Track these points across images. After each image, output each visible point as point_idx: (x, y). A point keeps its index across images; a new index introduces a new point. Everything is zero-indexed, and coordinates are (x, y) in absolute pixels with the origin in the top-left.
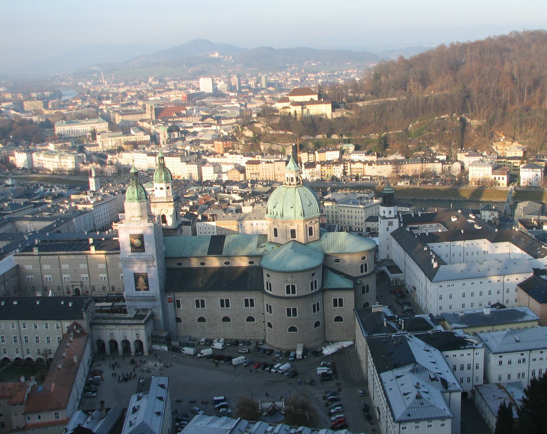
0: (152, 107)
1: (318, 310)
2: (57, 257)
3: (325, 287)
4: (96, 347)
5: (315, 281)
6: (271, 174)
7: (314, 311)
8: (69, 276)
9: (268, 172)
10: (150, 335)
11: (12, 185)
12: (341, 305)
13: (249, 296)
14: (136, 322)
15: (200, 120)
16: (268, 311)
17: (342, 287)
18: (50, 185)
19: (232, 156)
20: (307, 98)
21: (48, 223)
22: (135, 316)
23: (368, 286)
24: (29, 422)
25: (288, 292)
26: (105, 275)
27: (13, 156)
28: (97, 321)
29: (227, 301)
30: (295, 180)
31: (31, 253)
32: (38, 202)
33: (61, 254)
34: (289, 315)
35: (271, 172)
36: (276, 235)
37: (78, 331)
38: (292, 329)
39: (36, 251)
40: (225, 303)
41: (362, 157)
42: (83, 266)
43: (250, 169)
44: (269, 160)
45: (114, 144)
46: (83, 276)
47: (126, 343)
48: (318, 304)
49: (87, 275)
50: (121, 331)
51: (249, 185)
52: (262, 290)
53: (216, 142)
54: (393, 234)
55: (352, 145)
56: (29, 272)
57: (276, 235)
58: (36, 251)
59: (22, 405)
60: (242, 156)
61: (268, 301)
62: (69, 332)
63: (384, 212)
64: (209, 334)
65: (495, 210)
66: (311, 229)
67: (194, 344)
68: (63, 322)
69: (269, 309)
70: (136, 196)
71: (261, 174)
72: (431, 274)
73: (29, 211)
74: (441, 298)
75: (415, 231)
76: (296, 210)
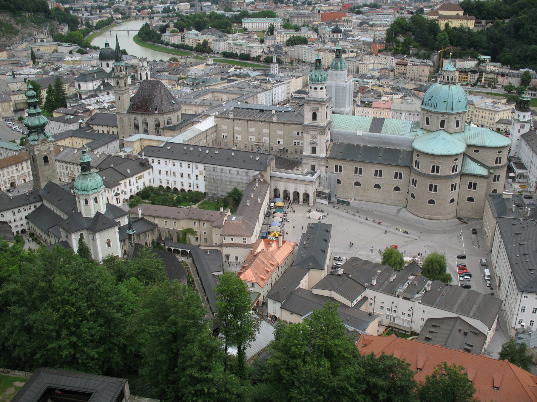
1: (455, 189)
2: (246, 122)
3: (463, 172)
4: (273, 193)
5: (457, 166)
6: (416, 74)
7: (452, 190)
8: (254, 137)
9: (413, 73)
10: (315, 191)
11: (212, 65)
12: (475, 188)
15: (357, 26)
16: (413, 184)
18: (239, 67)
19: (385, 56)
20: (454, 13)
23: (499, 176)
24: (224, 241)
25: (433, 171)
29: (380, 172)
33: (250, 120)
34: (430, 189)
35: (416, 74)
36: (427, 123)
37: (262, 180)
40: (378, 173)
42: (266, 131)
45: (288, 39)
46: (264, 138)
47: (296, 194)
48: (456, 184)
49: (268, 139)
55: (488, 57)
56: (224, 131)
57: (427, 123)
58: (231, 116)
59: (220, 228)
63: (519, 116)
64: (361, 196)
66: (458, 122)
67: (349, 202)
69: (415, 183)
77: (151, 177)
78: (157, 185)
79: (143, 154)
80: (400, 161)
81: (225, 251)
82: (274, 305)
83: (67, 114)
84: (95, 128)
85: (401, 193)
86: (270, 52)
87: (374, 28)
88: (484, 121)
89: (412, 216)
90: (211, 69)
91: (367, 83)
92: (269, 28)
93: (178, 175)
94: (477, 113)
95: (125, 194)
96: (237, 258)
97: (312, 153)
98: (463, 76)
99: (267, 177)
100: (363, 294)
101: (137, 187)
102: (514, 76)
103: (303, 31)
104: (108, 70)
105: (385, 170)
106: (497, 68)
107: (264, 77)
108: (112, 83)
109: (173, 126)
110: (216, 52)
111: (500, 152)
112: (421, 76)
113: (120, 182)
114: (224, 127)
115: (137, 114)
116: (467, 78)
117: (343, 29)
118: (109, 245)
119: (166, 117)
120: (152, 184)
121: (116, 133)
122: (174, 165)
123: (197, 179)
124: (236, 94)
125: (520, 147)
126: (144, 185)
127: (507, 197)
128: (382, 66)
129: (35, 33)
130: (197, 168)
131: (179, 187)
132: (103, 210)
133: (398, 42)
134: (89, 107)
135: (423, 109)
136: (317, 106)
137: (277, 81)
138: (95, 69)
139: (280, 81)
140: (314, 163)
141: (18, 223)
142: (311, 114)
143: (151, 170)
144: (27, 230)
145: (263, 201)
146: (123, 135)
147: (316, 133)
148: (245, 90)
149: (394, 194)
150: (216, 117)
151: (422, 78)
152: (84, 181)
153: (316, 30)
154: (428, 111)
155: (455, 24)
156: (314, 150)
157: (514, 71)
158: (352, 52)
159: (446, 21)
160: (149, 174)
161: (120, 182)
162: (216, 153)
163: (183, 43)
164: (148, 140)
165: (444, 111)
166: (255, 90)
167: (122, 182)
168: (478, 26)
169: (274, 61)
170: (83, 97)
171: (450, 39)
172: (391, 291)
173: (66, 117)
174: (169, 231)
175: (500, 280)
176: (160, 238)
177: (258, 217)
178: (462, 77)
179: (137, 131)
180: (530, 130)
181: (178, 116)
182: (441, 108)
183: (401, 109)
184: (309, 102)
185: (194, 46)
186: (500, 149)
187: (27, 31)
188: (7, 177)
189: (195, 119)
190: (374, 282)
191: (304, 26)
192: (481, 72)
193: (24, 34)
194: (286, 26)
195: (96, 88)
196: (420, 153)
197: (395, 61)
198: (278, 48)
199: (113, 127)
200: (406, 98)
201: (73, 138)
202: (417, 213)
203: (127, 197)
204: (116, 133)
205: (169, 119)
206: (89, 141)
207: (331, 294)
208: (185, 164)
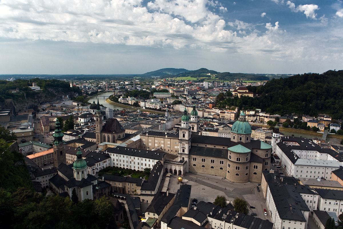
0: (187, 90)
1: (248, 169)
2: (154, 138)
4: (165, 170)
5: (248, 158)
7: (246, 169)
11: (139, 112)
13: (222, 160)
20: (244, 91)
21: (151, 126)
22: (180, 161)
23: (267, 162)
24: (142, 193)
25: (237, 160)
26: (170, 146)
27: (140, 102)
28: (167, 161)
29: (214, 161)
33: (155, 137)
34: (236, 169)
36: (234, 139)
37: (160, 164)
38: (237, 175)
39: (147, 135)
40: (213, 161)
41: (264, 115)
42: (163, 142)
44: (229, 112)
45: (173, 101)
47: (175, 171)
48: (248, 166)
50: (174, 166)
51: (222, 120)
52: (227, 158)
53: (210, 104)
54: (277, 144)
57: (234, 139)
58: (147, 135)
60: (219, 110)
61: (228, 163)
63: (275, 135)
65: (319, 140)
66: (248, 138)
68: (155, 160)
70: (185, 119)
71: (225, 117)
72: (294, 161)
73: (145, 121)
74: (297, 171)
77: (110, 162)
78: (112, 165)
79: (107, 151)
80: (222, 156)
81: (142, 198)
82: (164, 225)
84: (86, 139)
86: (166, 107)
87: (211, 97)
91: (207, 121)
93: (122, 161)
94: (256, 134)
95: (97, 170)
98: (250, 118)
99: (162, 162)
101: (103, 166)
102: (271, 117)
103: (180, 98)
104: (94, 113)
105: (215, 159)
107: (162, 118)
108: (95, 119)
109: (122, 139)
111: (267, 152)
113: (95, 164)
115: (105, 133)
117: (197, 97)
118: (87, 194)
119: (118, 135)
120: (110, 165)
121: (95, 141)
123: (131, 163)
124: (150, 125)
125: (276, 149)
126: (106, 165)
127: (272, 172)
128: (214, 113)
129: (63, 96)
131: (122, 167)
132: (86, 177)
134: (83, 129)
136: (185, 131)
137: (168, 120)
138: (88, 112)
139: (169, 120)
140: (183, 157)
141: (45, 183)
142: (182, 134)
143: (110, 159)
144: (49, 186)
145: (160, 174)
147: (185, 143)
151: (232, 119)
153: (185, 98)
154: (234, 133)
158: (201, 107)
159: (241, 94)
160: (109, 161)
161: (95, 164)
162: (140, 151)
166: (158, 123)
167: (96, 164)
169: (167, 111)
170: (82, 125)
171: (243, 102)
172: (219, 218)
174: (116, 188)
176: (111, 191)
177: (157, 182)
179: (105, 141)
180: (280, 141)
181: (124, 134)
182: (240, 132)
184: (182, 129)
185: (133, 104)
186: (267, 150)
187: (60, 96)
189: (131, 136)
190: (211, 213)
191: (180, 96)
192: (257, 116)
193: (58, 97)
194: (173, 96)
195: (88, 121)
197: (220, 111)
198: (169, 105)
199: (94, 138)
200: (225, 127)
201: (76, 143)
203: (98, 171)
204: (95, 141)
205: (120, 135)
206: (83, 145)
208: (125, 156)
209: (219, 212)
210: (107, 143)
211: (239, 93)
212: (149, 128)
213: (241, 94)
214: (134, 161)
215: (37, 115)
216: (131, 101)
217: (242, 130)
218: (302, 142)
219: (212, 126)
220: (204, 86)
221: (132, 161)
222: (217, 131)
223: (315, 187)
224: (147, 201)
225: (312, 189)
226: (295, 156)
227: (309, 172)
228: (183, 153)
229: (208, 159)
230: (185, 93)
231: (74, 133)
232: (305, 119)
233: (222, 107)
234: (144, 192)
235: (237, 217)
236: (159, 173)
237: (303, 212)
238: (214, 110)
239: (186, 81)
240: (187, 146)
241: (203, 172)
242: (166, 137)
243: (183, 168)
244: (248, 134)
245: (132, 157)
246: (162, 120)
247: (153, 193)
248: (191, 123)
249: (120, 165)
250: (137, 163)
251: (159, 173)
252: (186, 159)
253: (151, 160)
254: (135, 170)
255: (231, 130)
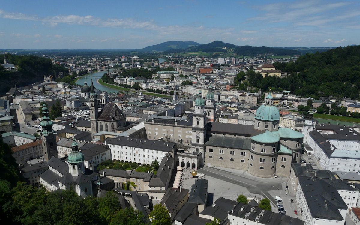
1: (274, 161)
2: (161, 126)
7: (272, 161)
12: (285, 160)
13: (243, 151)
14: (194, 155)
17: (286, 152)
19: (233, 91)
20: (270, 69)
25: (262, 151)
30: (270, 102)
31: (150, 123)
32: (152, 103)
34: (261, 161)
38: (262, 168)
39: (153, 122)
42: (172, 130)
43: (241, 99)
44: (250, 95)
45: (182, 82)
46: (171, 134)
56: (149, 130)
58: (153, 122)
61: (251, 154)
62: (166, 156)
63: (307, 122)
64: (223, 165)
70: (200, 102)
75: (321, 133)
76: (270, 116)
79: (105, 142)
81: (150, 195)
83: (63, 120)
84: (79, 128)
85: (245, 163)
86: (173, 89)
87: (228, 77)
88: (288, 125)
89: (251, 175)
90: (141, 98)
92: (172, 77)
93: (124, 153)
94: (284, 121)
96: (157, 198)
97: (197, 142)
98: (276, 102)
100: (227, 218)
101: (102, 160)
104: (86, 97)
105: (236, 151)
106: (294, 97)
107: (170, 102)
110: (144, 89)
112: (253, 102)
114: (149, 128)
116: (278, 103)
117: (211, 77)
121: (90, 131)
122: (122, 148)
126: (106, 159)
128: (232, 97)
130: (135, 149)
131: (125, 160)
133: (240, 84)
135: (256, 119)
142: (196, 121)
146: (94, 132)
147: (200, 131)
148: (160, 108)
149: (241, 164)
150: (144, 123)
151: (254, 103)
152: (74, 156)
153: (197, 78)
155: (272, 74)
156: (198, 141)
157: (303, 99)
159: (266, 73)
161: (93, 157)
162: (145, 142)
163: (126, 84)
164: (108, 135)
165: (267, 120)
167: (94, 157)
168: (283, 76)
169: (175, 94)
172: (242, 216)
173: (62, 122)
175: (302, 210)
178: (275, 102)
179: (102, 130)
181: (124, 122)
183: (243, 119)
184: (195, 116)
185: (132, 86)
188: (28, 154)
191: (190, 75)
192: (286, 99)
194: (181, 76)
196: (254, 142)
197: (240, 94)
198: (177, 87)
202: (254, 174)
204: (90, 131)
206: (75, 135)
207: (210, 217)
208: (128, 148)
209: (242, 209)
210: (104, 132)
211: (264, 71)
212: (154, 114)
213: (266, 73)
214: (139, 152)
215: (13, 99)
216: (129, 83)
217: (269, 117)
218: (341, 130)
219: (231, 112)
220: (219, 63)
221: (137, 153)
222: (236, 117)
223: (354, 182)
224: (157, 198)
225: (351, 184)
226: (331, 147)
227: (348, 165)
228: (197, 143)
229: (227, 151)
230: (196, 72)
231: (64, 122)
232: (345, 103)
233: (242, 89)
234: (152, 188)
235: (263, 215)
236: (169, 166)
237: (339, 210)
238: (232, 92)
239: (196, 57)
240: (201, 135)
241: (220, 165)
242: (176, 124)
243: (198, 161)
244: (275, 121)
245: (137, 149)
246: (169, 105)
247: (164, 189)
248: (206, 108)
249: (123, 158)
250: (143, 156)
251: (169, 166)
252: (201, 150)
253: (159, 152)
254: (140, 164)
255: (256, 116)
